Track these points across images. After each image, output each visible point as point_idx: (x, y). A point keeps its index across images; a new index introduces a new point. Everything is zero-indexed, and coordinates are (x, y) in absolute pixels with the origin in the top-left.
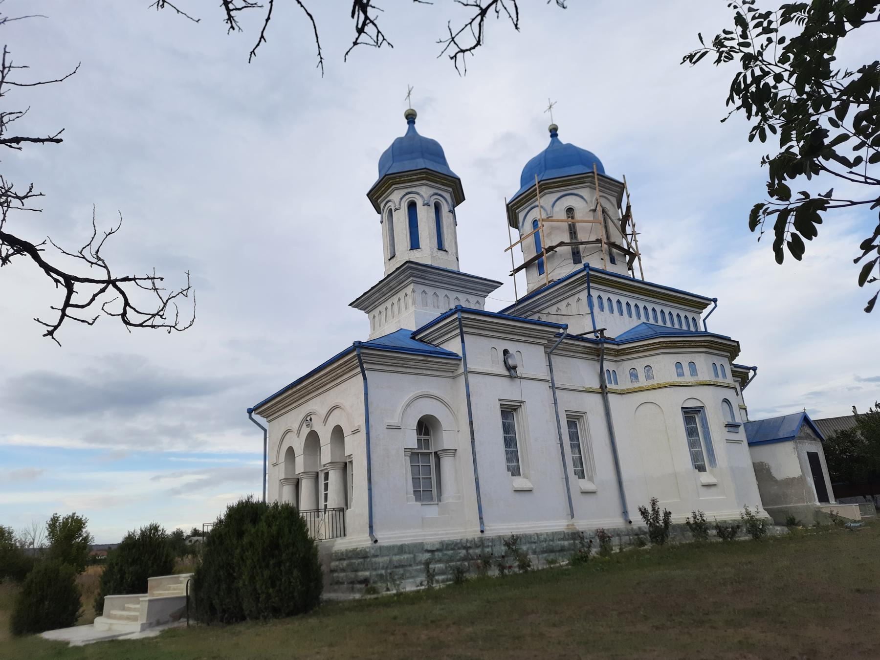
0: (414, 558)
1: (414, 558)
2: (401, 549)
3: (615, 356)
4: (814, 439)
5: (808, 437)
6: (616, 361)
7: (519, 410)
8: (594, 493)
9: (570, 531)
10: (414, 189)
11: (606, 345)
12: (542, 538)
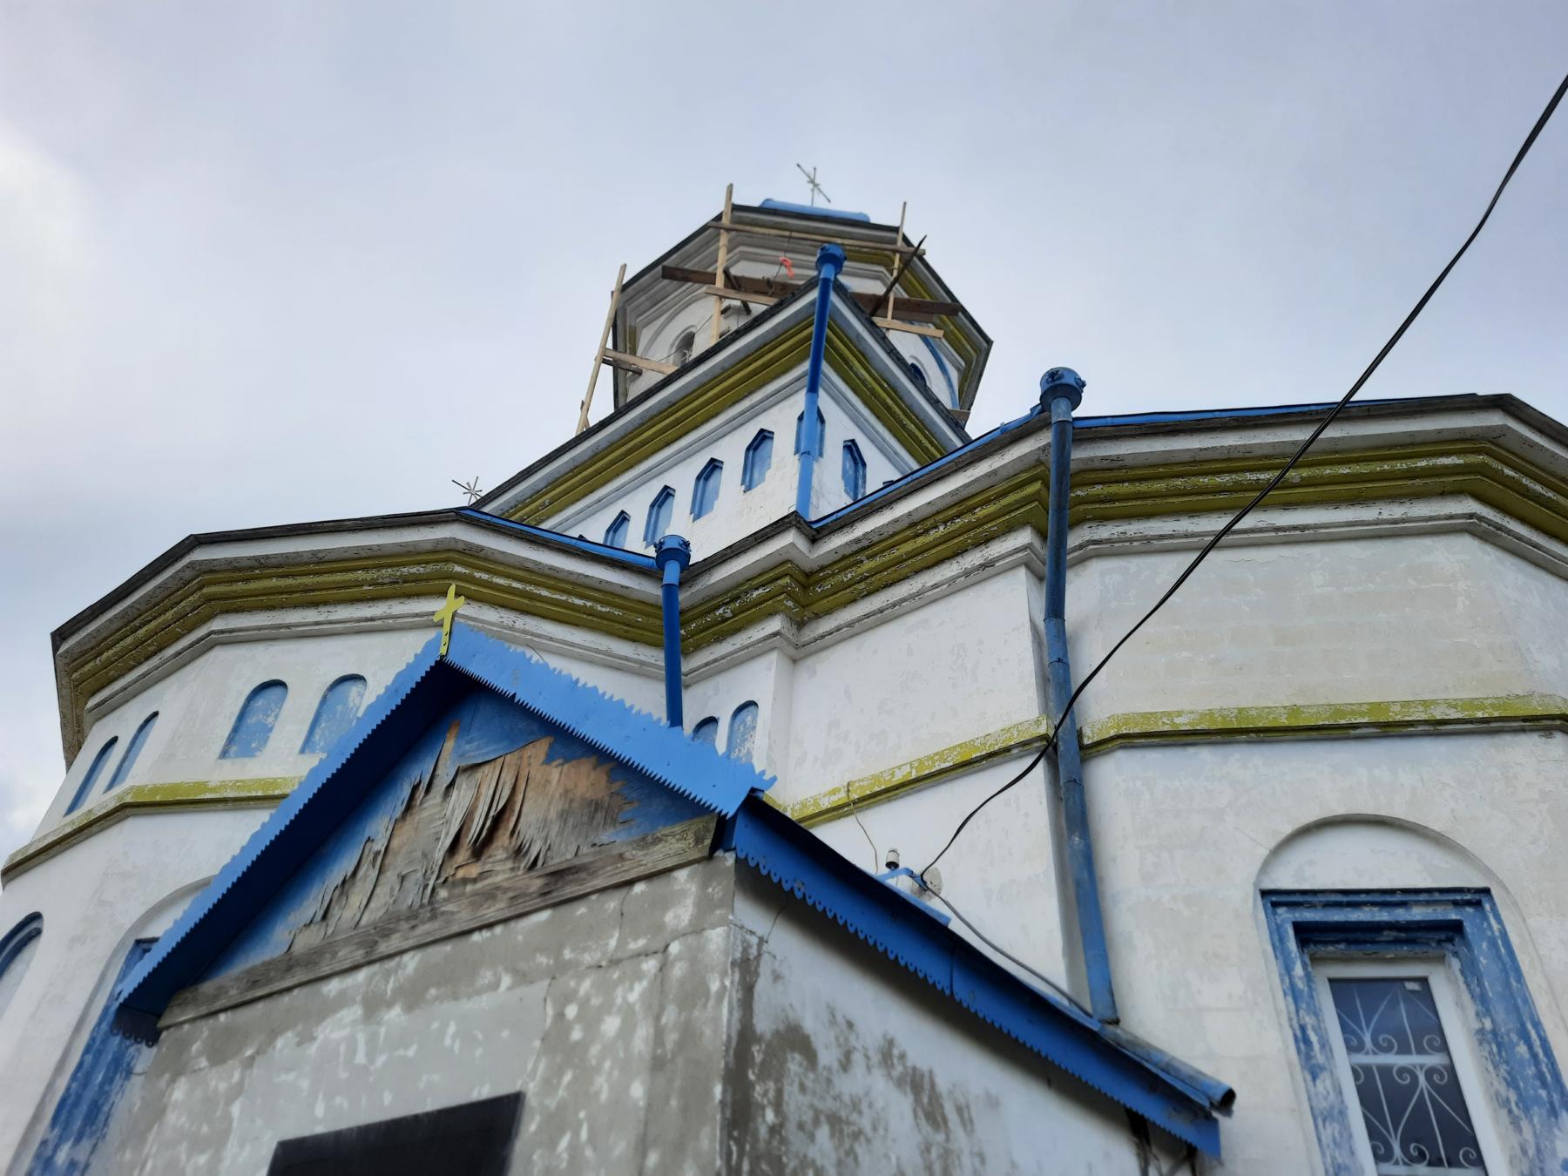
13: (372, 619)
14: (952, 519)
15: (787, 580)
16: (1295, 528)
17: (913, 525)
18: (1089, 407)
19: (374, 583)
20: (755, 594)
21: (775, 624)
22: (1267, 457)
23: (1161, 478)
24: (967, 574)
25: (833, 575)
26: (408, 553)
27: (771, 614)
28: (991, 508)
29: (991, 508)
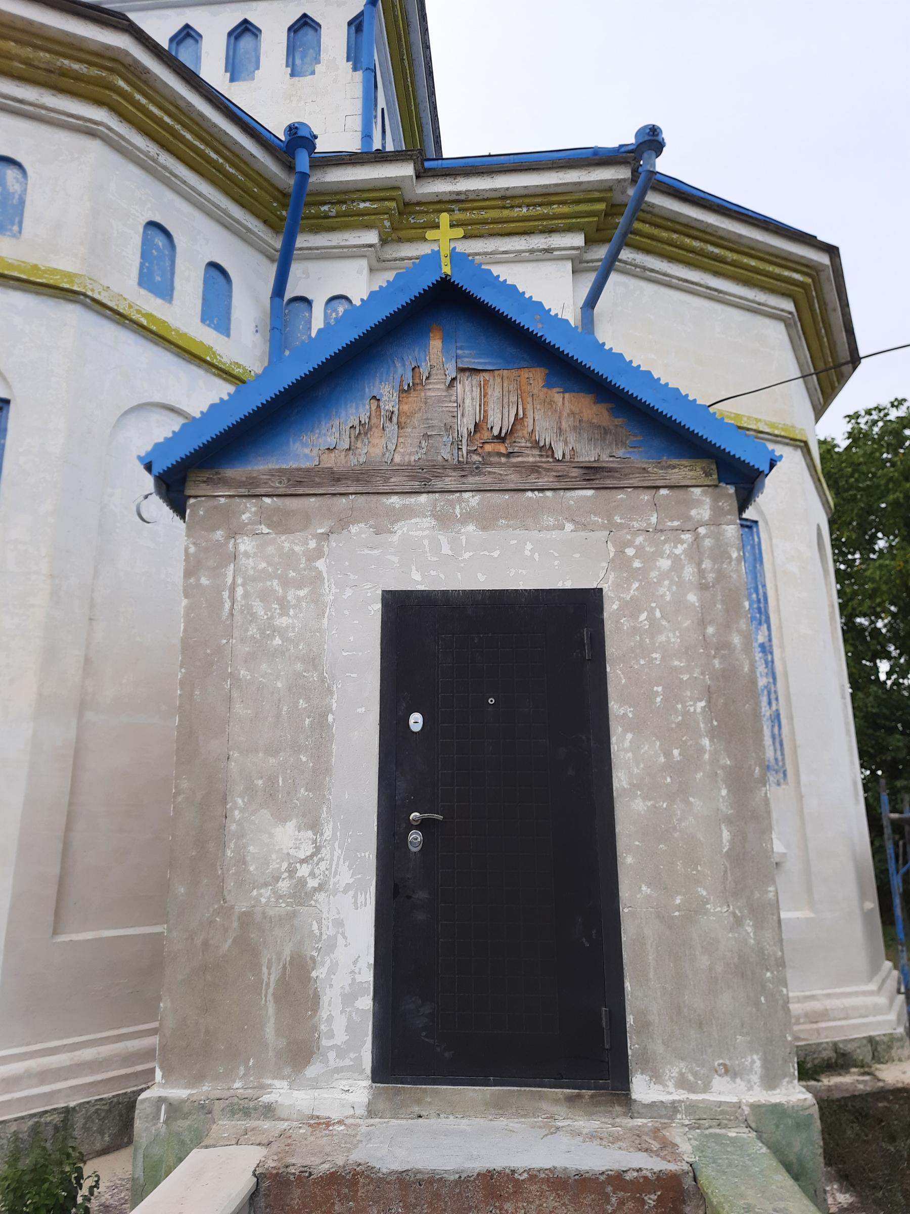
4: (592, 475)
5: (488, 463)
13: (21, 101)
14: (535, 205)
15: (393, 204)
16: (716, 290)
17: (504, 198)
18: (665, 165)
19: (27, 62)
20: (362, 205)
21: (372, 237)
22: (721, 238)
23: (666, 229)
24: (532, 251)
25: (427, 212)
26: (70, 46)
27: (368, 227)
28: (565, 209)
29: (565, 209)
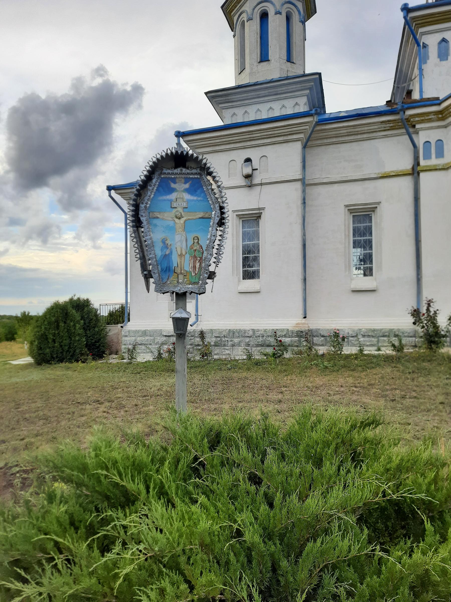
0: (154, 339)
1: (154, 339)
2: (145, 333)
3: (443, 119)
6: (445, 127)
7: (262, 216)
8: (374, 291)
9: (297, 329)
10: (241, 11)
11: (410, 112)
12: (257, 334)
